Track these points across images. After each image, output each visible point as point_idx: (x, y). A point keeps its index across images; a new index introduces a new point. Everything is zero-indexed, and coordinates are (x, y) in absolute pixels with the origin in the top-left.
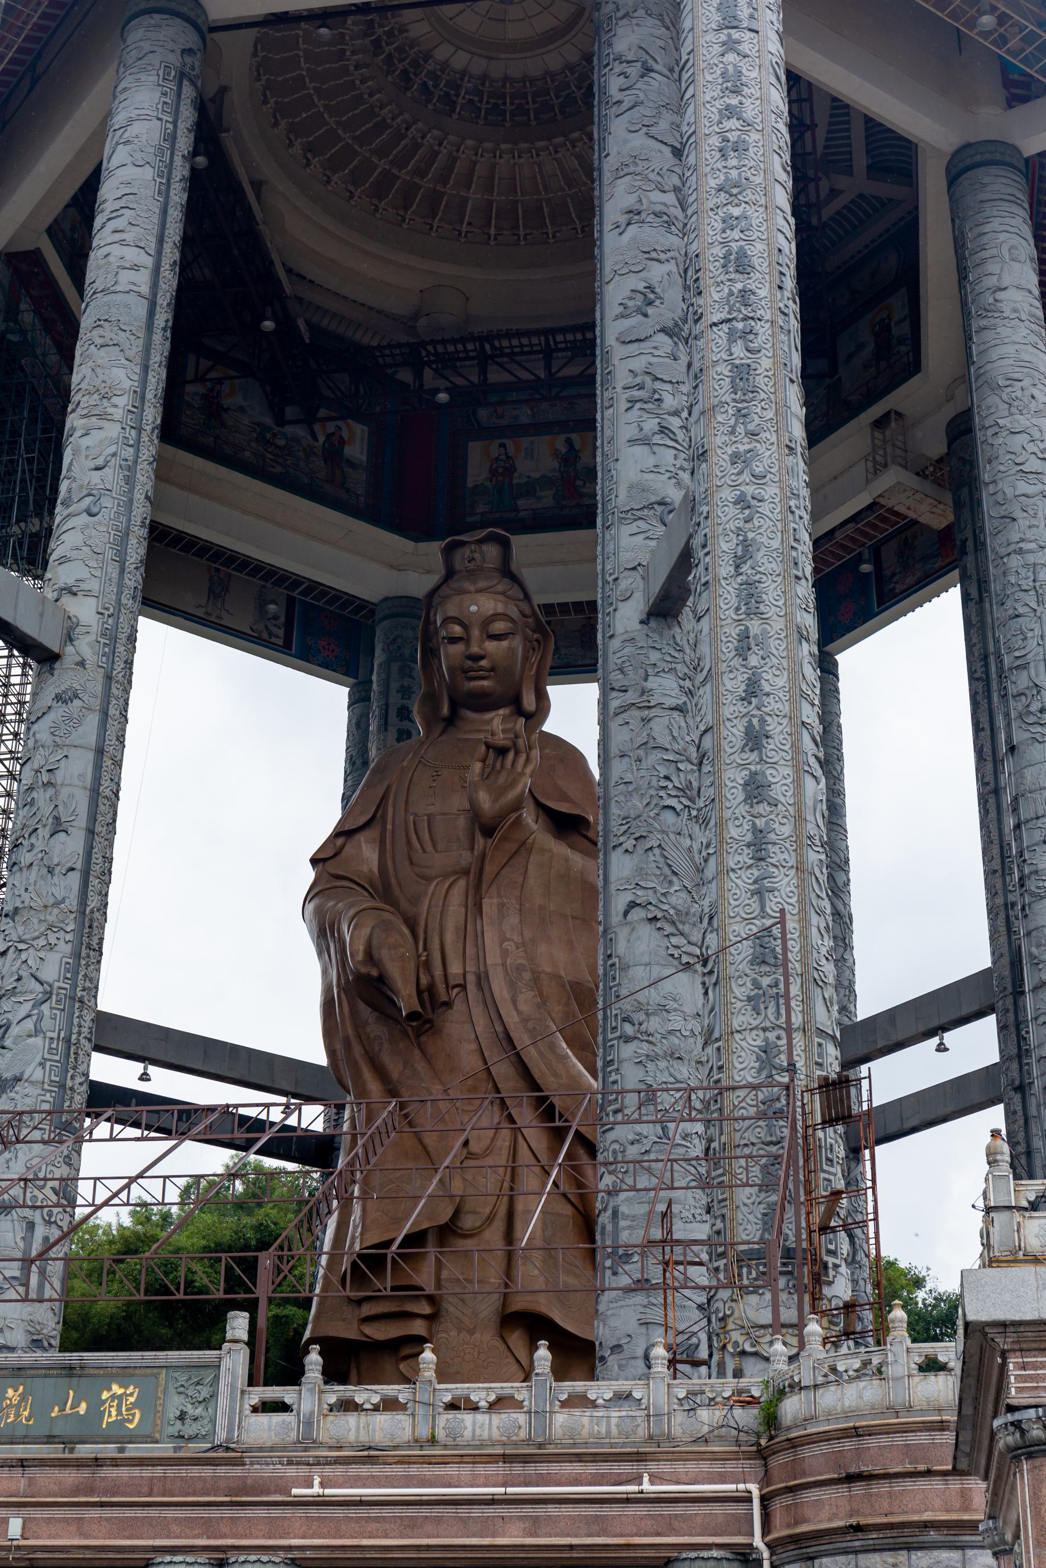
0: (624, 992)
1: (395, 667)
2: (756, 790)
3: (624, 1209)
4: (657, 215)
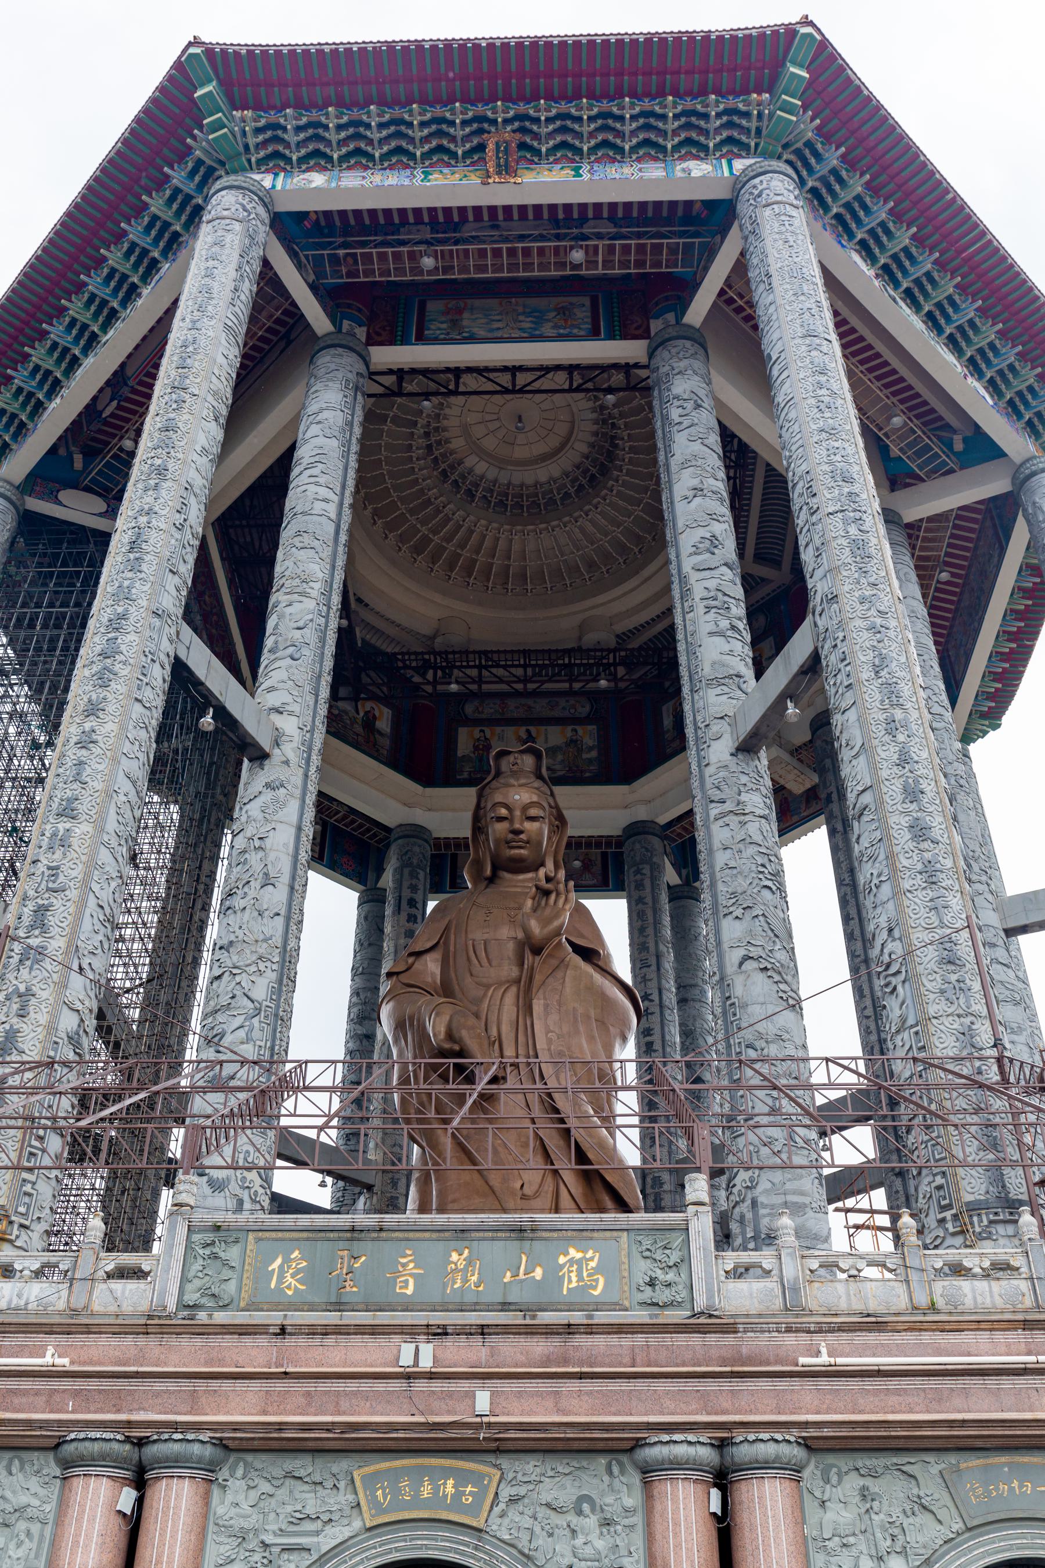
0: (744, 1025)
1: (406, 871)
2: (920, 832)
3: (762, 1199)
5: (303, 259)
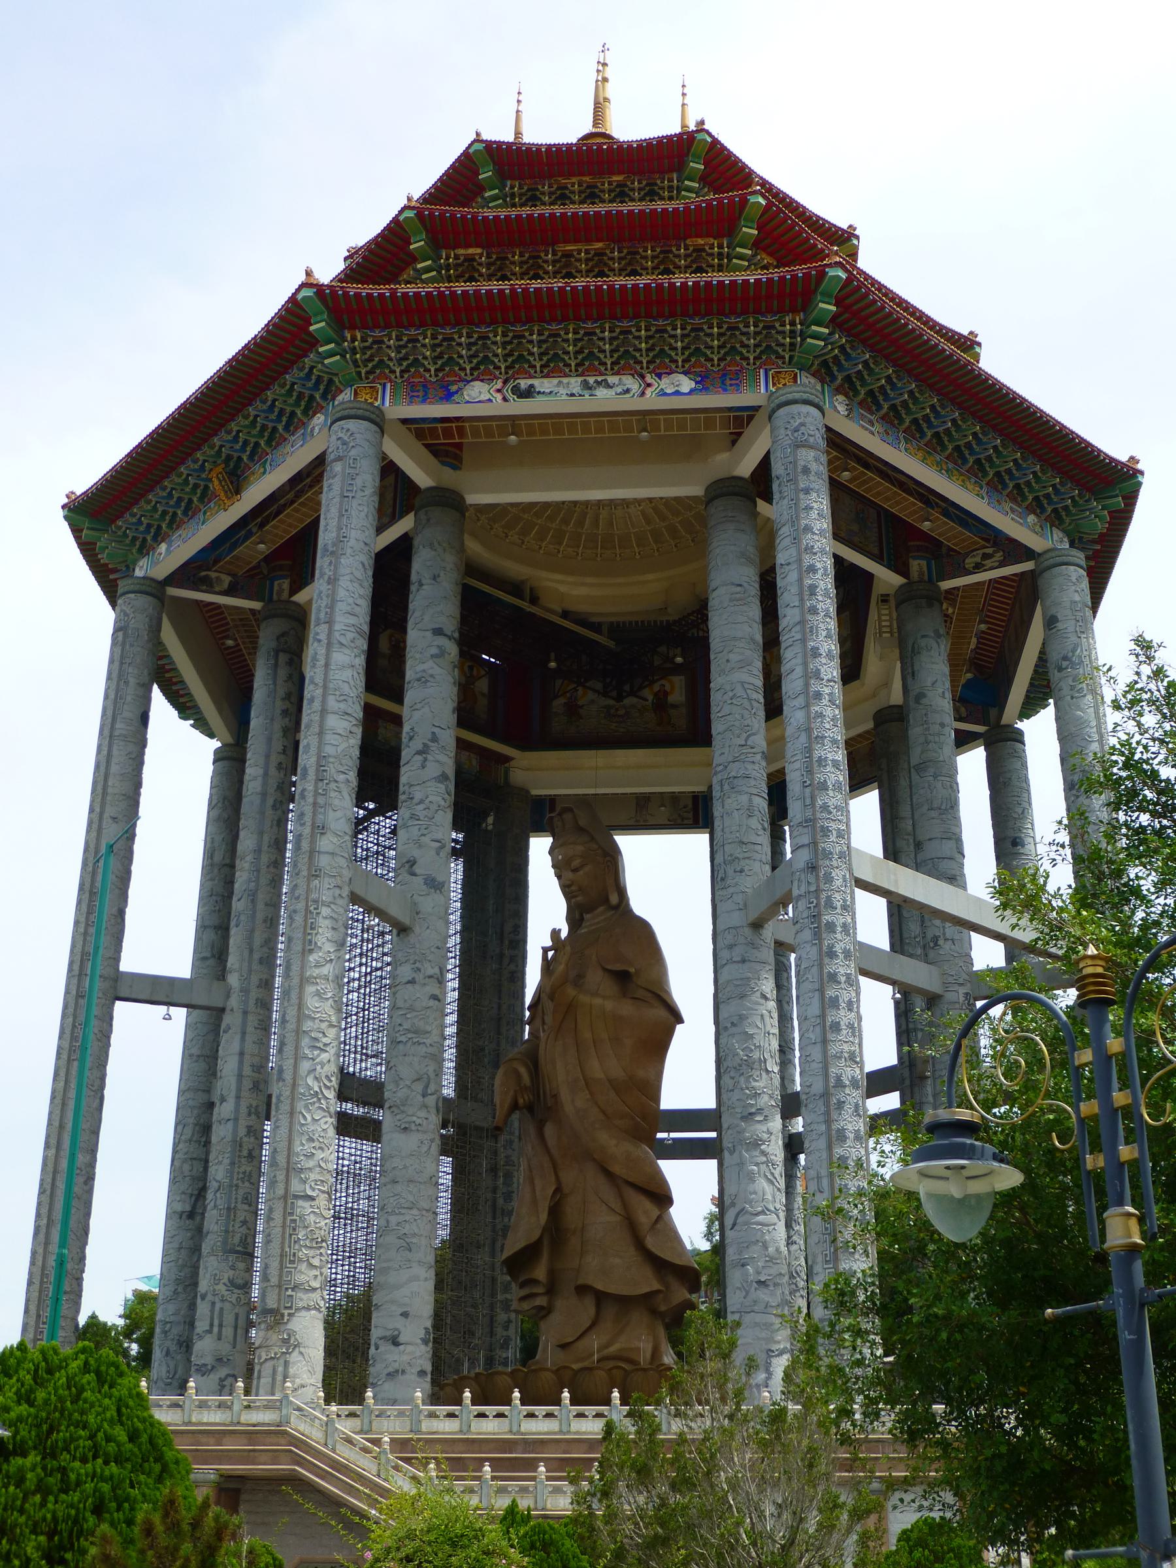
4: (419, 680)
5: (213, 575)
